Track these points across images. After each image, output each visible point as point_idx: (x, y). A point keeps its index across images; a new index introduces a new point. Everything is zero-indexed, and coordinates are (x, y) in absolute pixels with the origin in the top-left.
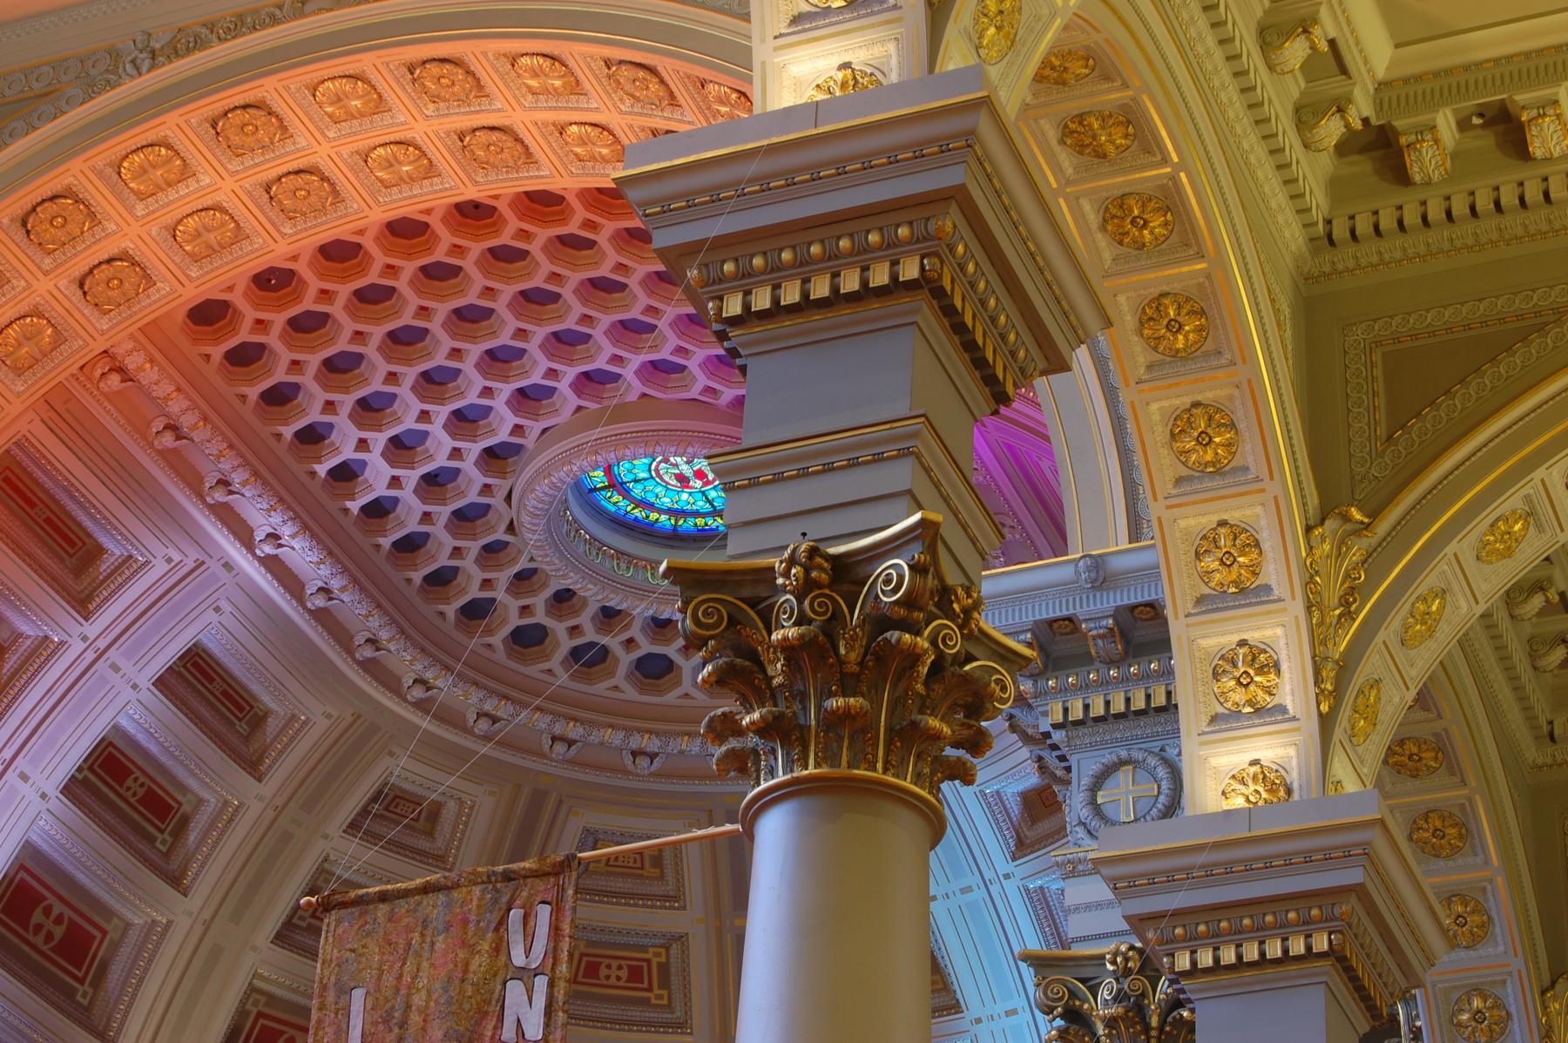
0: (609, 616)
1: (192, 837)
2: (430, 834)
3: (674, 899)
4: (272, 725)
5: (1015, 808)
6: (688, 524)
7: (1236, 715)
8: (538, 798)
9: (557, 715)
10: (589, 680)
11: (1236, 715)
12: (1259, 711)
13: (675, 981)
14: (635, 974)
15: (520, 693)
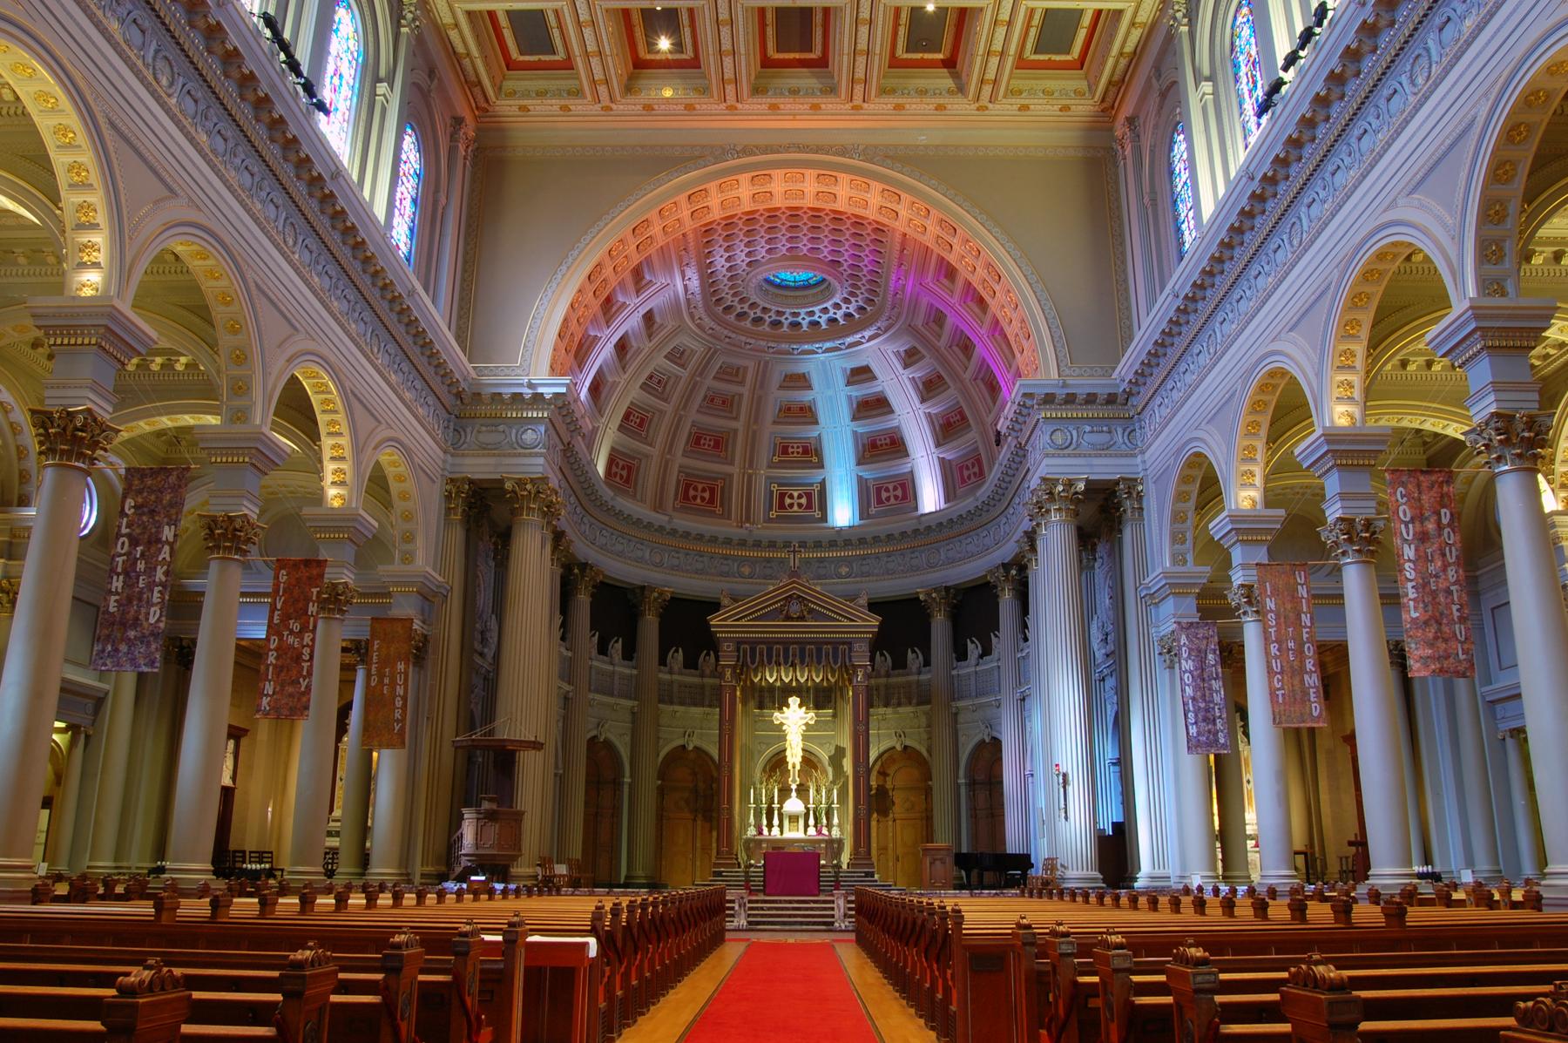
0: (753, 305)
1: (628, 357)
2: (680, 358)
3: (742, 383)
4: (656, 326)
5: (848, 372)
6: (784, 283)
7: (1245, 485)
8: (715, 352)
9: (747, 337)
10: (739, 321)
11: (1245, 485)
12: (1251, 485)
13: (735, 406)
14: (724, 402)
15: (736, 329)
